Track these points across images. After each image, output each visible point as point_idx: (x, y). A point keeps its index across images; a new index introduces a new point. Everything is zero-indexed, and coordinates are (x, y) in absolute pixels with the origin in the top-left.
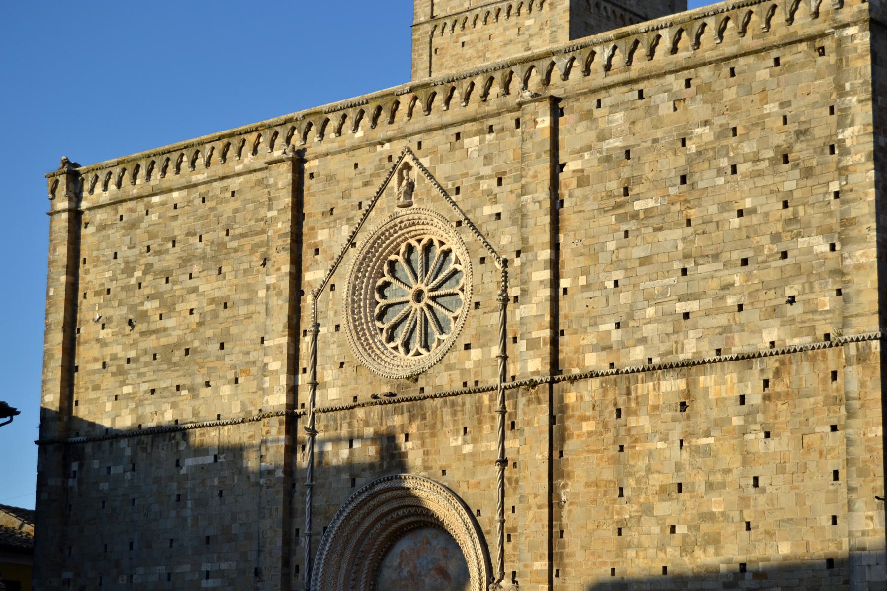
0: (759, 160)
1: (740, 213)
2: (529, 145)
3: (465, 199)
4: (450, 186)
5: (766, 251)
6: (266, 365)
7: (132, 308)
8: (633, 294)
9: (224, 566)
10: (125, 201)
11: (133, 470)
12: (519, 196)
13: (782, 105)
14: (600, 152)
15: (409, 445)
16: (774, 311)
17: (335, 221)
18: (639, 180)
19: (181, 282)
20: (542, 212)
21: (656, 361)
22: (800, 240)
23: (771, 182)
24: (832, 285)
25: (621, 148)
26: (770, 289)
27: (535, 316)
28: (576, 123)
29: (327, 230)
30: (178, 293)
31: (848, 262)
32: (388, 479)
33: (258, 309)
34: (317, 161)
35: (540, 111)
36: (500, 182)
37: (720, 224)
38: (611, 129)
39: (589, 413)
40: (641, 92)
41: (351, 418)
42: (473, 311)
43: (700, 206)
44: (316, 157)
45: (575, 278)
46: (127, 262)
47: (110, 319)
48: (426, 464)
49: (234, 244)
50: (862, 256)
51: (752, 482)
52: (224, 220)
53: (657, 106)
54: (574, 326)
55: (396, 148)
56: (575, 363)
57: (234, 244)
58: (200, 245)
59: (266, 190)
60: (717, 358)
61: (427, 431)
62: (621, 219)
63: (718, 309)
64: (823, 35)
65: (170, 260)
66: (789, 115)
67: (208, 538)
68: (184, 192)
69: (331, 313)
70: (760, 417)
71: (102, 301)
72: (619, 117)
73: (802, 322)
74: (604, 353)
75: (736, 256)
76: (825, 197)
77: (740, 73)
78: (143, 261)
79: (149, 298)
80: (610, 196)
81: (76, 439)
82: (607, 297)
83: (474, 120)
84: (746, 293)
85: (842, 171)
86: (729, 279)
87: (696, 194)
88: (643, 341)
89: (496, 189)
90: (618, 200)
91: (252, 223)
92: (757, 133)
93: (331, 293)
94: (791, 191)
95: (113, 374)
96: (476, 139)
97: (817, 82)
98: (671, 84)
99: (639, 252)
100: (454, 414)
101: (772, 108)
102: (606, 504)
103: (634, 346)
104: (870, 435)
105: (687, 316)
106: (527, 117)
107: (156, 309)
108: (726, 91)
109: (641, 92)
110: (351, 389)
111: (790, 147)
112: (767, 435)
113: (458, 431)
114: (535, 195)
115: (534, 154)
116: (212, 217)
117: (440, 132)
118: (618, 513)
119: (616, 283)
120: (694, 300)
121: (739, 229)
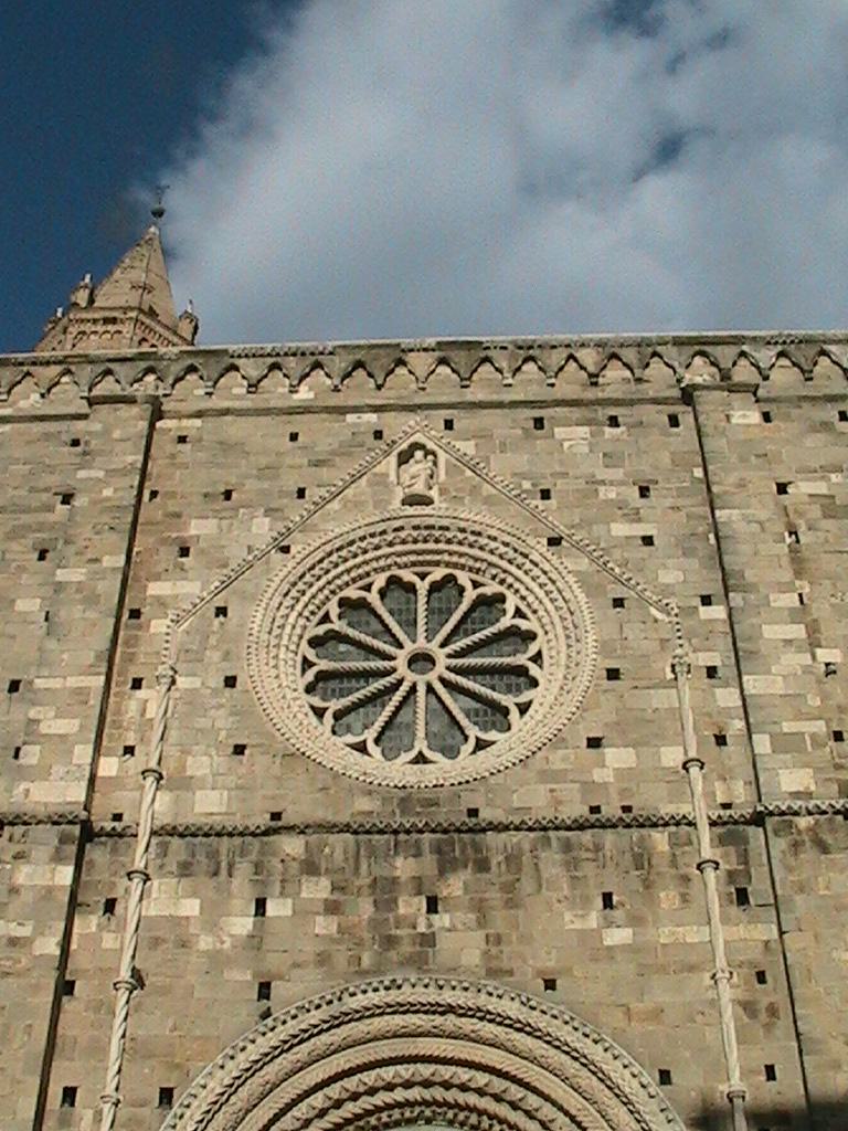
15: (442, 920)
41: (262, 853)
48: (494, 964)
61: (494, 896)
69: (216, 656)
100: (572, 864)
110: (264, 797)
113: (586, 901)
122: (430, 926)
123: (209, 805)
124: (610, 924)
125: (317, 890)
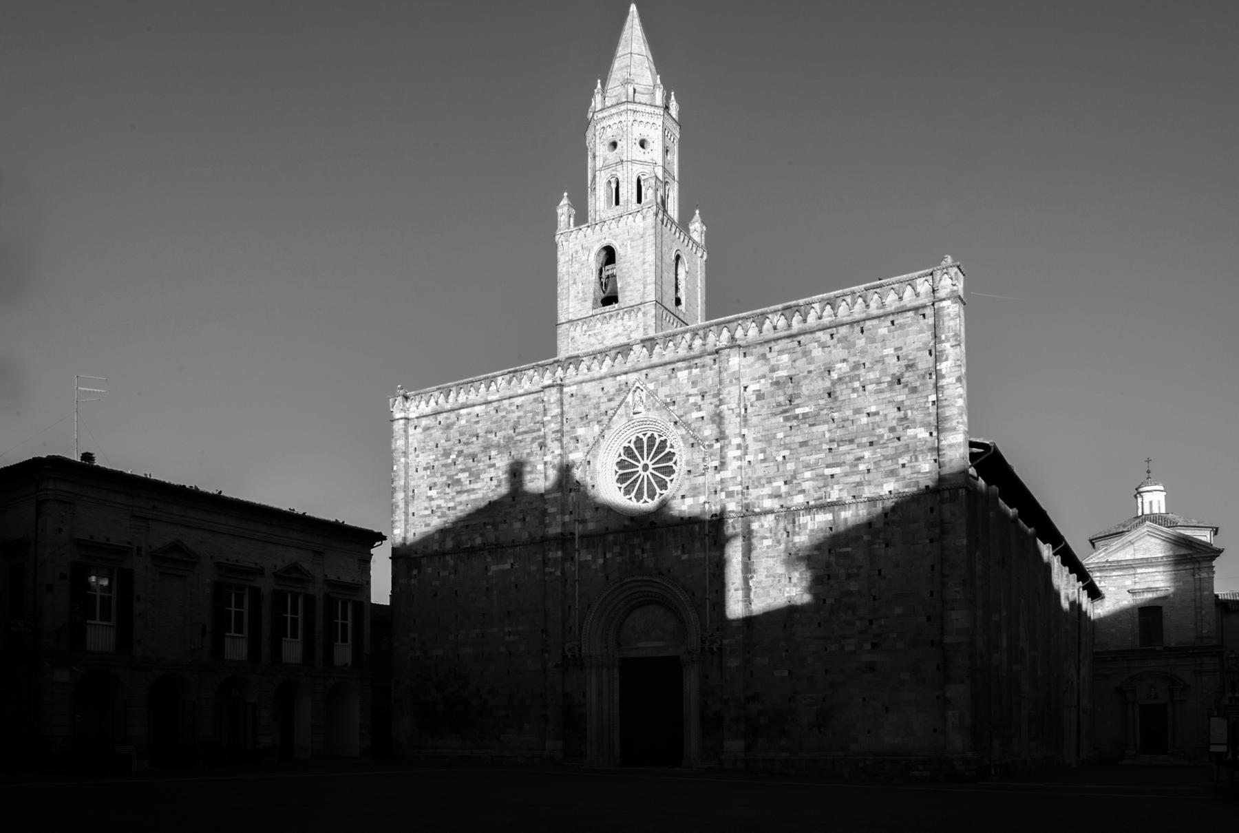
0: (881, 383)
1: (868, 414)
2: (725, 375)
3: (679, 408)
4: (668, 400)
5: (886, 437)
6: (547, 509)
7: (450, 477)
8: (795, 464)
9: (520, 628)
10: (442, 412)
11: (456, 573)
12: (717, 406)
13: (896, 349)
14: (772, 379)
15: (645, 555)
16: (892, 473)
17: (589, 423)
18: (798, 396)
19: (484, 461)
20: (734, 415)
21: (812, 503)
22: (908, 430)
23: (889, 395)
24: (930, 457)
25: (786, 377)
26: (888, 460)
27: (731, 478)
28: (755, 361)
29: (584, 428)
30: (481, 468)
31: (943, 443)
32: (633, 576)
33: (538, 476)
34: (576, 386)
35: (732, 355)
36: (703, 396)
37: (854, 421)
38: (778, 365)
39: (768, 535)
40: (799, 342)
42: (687, 476)
43: (840, 411)
44: (575, 384)
45: (756, 455)
46: (445, 450)
47: (435, 484)
49: (520, 438)
50: (952, 439)
51: (877, 572)
52: (511, 423)
53: (811, 351)
54: (756, 484)
55: (632, 377)
56: (757, 506)
57: (520, 438)
58: (495, 439)
59: (541, 405)
60: (854, 501)
62: (787, 419)
63: (853, 472)
64: (924, 307)
65: (475, 448)
66: (901, 355)
67: (509, 612)
68: (484, 406)
70: (882, 535)
71: (429, 473)
72: (785, 358)
73: (911, 479)
74: (777, 499)
75: (865, 440)
76: (925, 405)
77: (867, 330)
78: (456, 449)
79: (463, 471)
80: (779, 405)
81: (416, 556)
82: (778, 466)
83: (684, 360)
84: (872, 462)
85: (937, 388)
86: (861, 454)
87: (838, 404)
88: (803, 491)
89: (700, 402)
90: (784, 408)
91: (532, 424)
92: (879, 366)
93: (588, 467)
94: (903, 401)
95: (439, 517)
96: (687, 372)
97: (920, 335)
98: (820, 337)
99: (799, 439)
101: (889, 351)
102: (780, 588)
103: (796, 495)
104: (958, 544)
105: (832, 476)
106: (722, 358)
107: (467, 477)
108: (858, 341)
109: (799, 342)
111: (902, 375)
112: (887, 545)
114: (729, 405)
115: (728, 380)
116: (503, 421)
117: (661, 368)
118: (788, 592)
119: (784, 457)
120: (838, 466)
121: (868, 424)
122: (642, 557)
123: (591, 526)
124: (683, 552)
125: (617, 549)
